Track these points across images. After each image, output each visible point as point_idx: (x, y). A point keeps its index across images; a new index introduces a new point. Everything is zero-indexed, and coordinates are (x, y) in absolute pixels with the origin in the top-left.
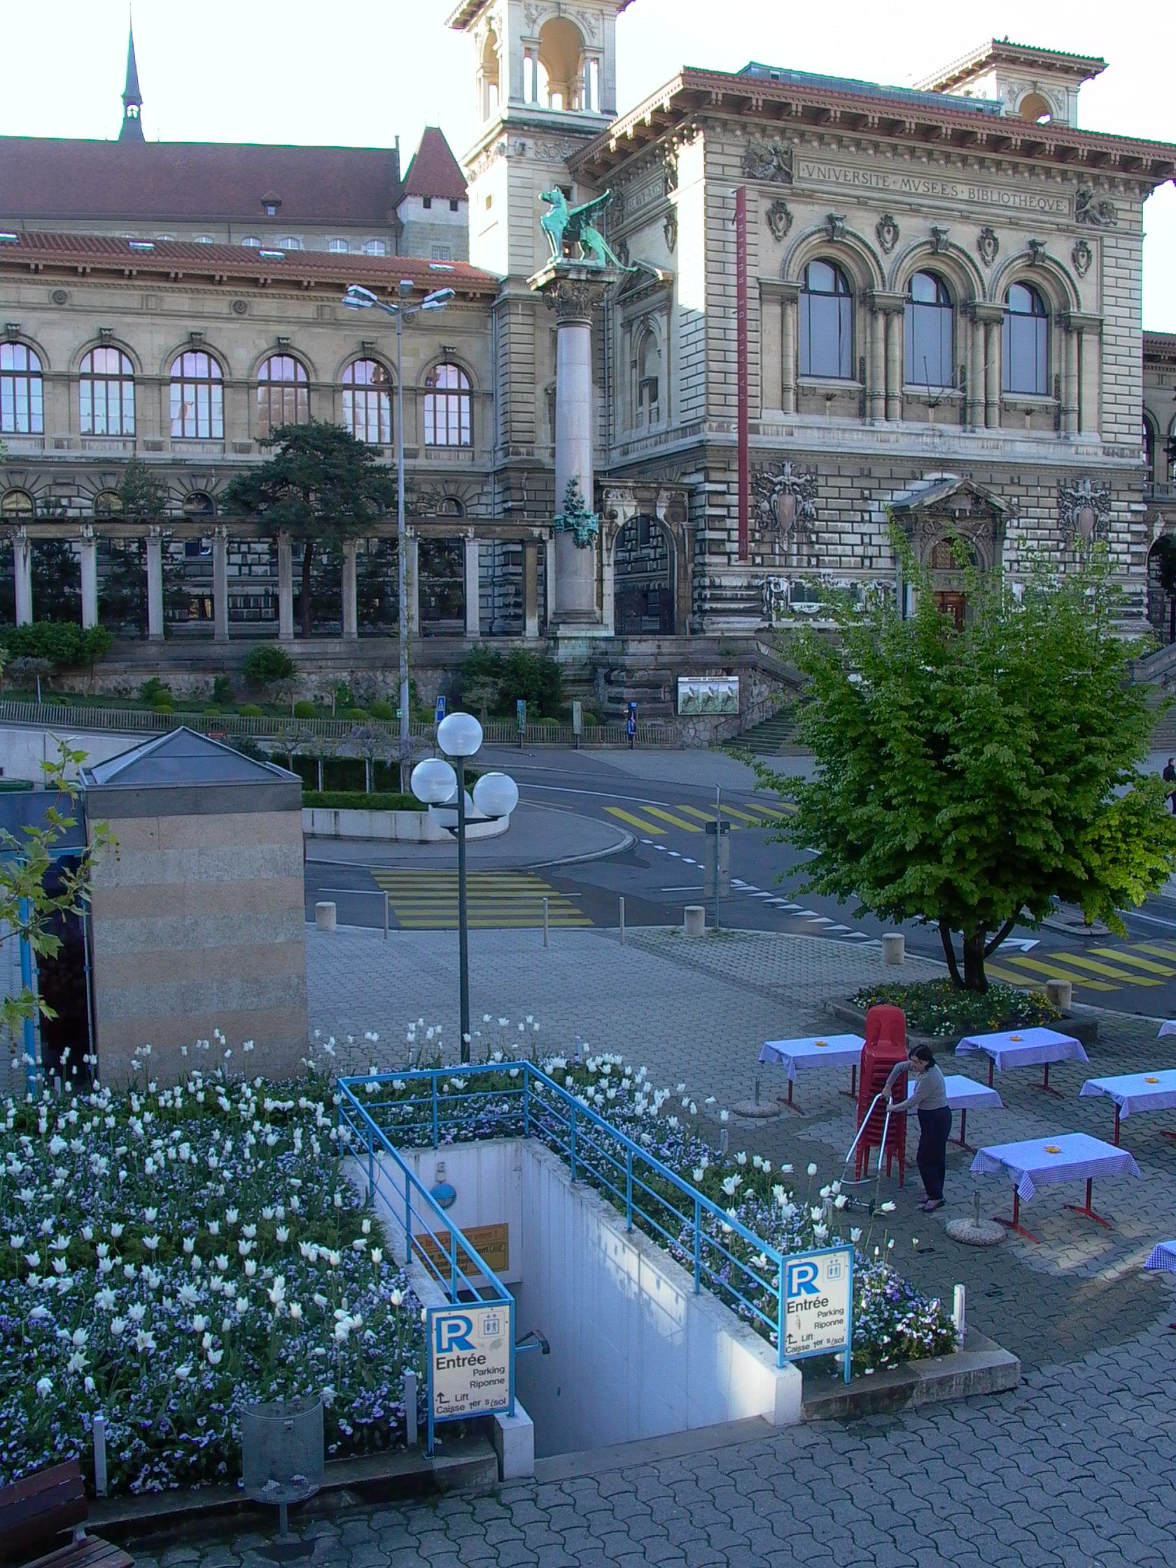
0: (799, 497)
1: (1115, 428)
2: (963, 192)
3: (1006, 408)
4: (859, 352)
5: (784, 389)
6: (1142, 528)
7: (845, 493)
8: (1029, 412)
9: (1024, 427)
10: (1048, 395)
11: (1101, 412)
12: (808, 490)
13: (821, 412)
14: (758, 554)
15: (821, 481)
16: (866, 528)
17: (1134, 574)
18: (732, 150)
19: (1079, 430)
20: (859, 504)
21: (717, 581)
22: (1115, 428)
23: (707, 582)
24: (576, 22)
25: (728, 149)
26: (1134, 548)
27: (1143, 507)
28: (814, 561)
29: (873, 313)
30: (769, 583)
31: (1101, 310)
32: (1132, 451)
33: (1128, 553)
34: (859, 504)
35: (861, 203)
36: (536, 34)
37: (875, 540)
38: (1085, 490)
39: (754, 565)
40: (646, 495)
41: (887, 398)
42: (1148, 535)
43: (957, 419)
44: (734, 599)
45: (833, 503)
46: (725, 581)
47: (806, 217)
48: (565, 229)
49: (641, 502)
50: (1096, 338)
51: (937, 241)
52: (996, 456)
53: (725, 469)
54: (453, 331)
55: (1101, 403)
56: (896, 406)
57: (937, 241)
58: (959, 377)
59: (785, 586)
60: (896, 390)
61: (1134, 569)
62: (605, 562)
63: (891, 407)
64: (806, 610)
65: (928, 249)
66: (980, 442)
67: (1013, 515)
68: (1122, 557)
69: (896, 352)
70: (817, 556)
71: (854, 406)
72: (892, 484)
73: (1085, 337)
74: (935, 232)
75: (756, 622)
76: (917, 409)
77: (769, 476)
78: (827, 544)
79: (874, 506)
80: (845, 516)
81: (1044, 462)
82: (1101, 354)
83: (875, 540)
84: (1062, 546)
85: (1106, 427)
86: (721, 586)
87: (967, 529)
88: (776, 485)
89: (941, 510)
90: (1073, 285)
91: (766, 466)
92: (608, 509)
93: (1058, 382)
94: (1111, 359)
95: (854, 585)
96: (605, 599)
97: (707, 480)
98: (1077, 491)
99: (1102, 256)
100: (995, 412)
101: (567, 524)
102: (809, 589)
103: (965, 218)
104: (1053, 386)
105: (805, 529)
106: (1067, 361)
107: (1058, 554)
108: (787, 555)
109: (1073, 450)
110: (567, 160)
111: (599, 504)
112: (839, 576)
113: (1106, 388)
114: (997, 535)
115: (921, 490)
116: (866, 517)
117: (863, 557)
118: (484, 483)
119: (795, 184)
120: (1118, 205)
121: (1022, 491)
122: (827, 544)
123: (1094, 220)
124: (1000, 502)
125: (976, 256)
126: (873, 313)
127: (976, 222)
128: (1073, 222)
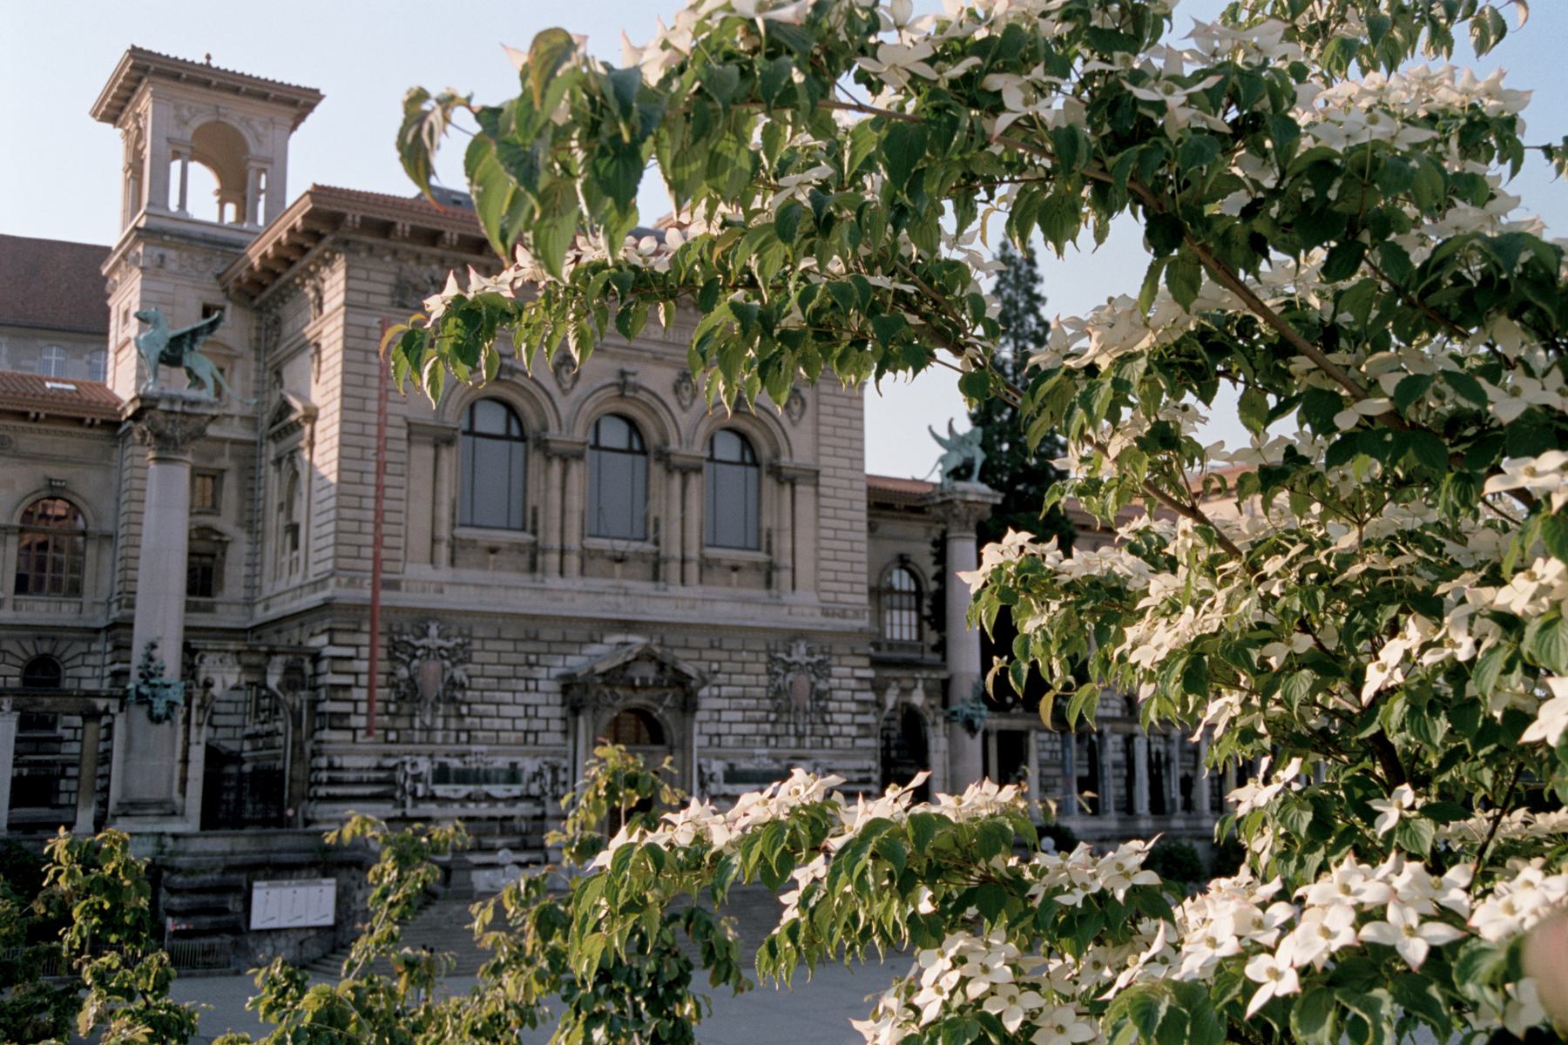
0: (447, 663)
1: (835, 586)
3: (706, 565)
4: (532, 500)
5: (434, 541)
6: (870, 696)
7: (506, 658)
8: (735, 569)
9: (729, 584)
10: (758, 549)
11: (818, 569)
12: (460, 655)
13: (483, 566)
14: (393, 729)
15: (476, 645)
16: (530, 698)
17: (861, 748)
18: (380, 277)
19: (794, 587)
20: (523, 671)
21: (337, 762)
22: (835, 586)
23: (323, 762)
24: (240, 128)
25: (373, 275)
26: (859, 719)
27: (870, 673)
28: (463, 737)
29: (548, 459)
30: (404, 763)
31: (817, 460)
32: (856, 612)
33: (852, 723)
34: (523, 671)
36: (188, 137)
37: (542, 712)
38: (799, 654)
39: (386, 741)
40: (254, 659)
41: (563, 552)
42: (880, 705)
43: (650, 574)
44: (359, 783)
45: (489, 670)
46: (348, 762)
48: (163, 353)
49: (247, 668)
50: (811, 490)
51: (624, 385)
52: (693, 617)
53: (355, 631)
54: (66, 461)
55: (818, 559)
56: (573, 562)
57: (624, 385)
58: (650, 529)
59: (424, 766)
60: (573, 542)
61: (859, 742)
62: (193, 738)
63: (566, 562)
64: (452, 795)
65: (614, 391)
67: (705, 683)
68: (846, 730)
69: (575, 501)
70: (468, 731)
71: (524, 560)
72: (565, 648)
73: (799, 488)
74: (623, 374)
75: (388, 809)
76: (600, 564)
77: (411, 639)
78: (481, 717)
79: (541, 673)
80: (505, 684)
81: (749, 623)
82: (818, 507)
83: (542, 712)
84: (772, 717)
85: (824, 585)
86: (341, 769)
87: (652, 699)
88: (417, 648)
89: (617, 676)
90: (784, 433)
91: (407, 627)
92: (201, 678)
93: (769, 536)
94: (830, 512)
95: (513, 765)
96: (189, 785)
97: (331, 643)
98: (789, 655)
99: (818, 403)
100: (693, 570)
101: (139, 695)
102: (457, 771)
103: (658, 359)
104: (764, 541)
105: (453, 700)
106: (779, 513)
107: (767, 728)
108: (430, 730)
109: (785, 610)
110: (218, 276)
111: (189, 670)
112: (495, 753)
113: (824, 543)
114: (688, 706)
115: (603, 654)
116: (532, 685)
117: (526, 732)
118: (90, 641)
121: (725, 655)
122: (481, 717)
124: (688, 668)
125: (671, 400)
126: (548, 459)
127: (672, 364)
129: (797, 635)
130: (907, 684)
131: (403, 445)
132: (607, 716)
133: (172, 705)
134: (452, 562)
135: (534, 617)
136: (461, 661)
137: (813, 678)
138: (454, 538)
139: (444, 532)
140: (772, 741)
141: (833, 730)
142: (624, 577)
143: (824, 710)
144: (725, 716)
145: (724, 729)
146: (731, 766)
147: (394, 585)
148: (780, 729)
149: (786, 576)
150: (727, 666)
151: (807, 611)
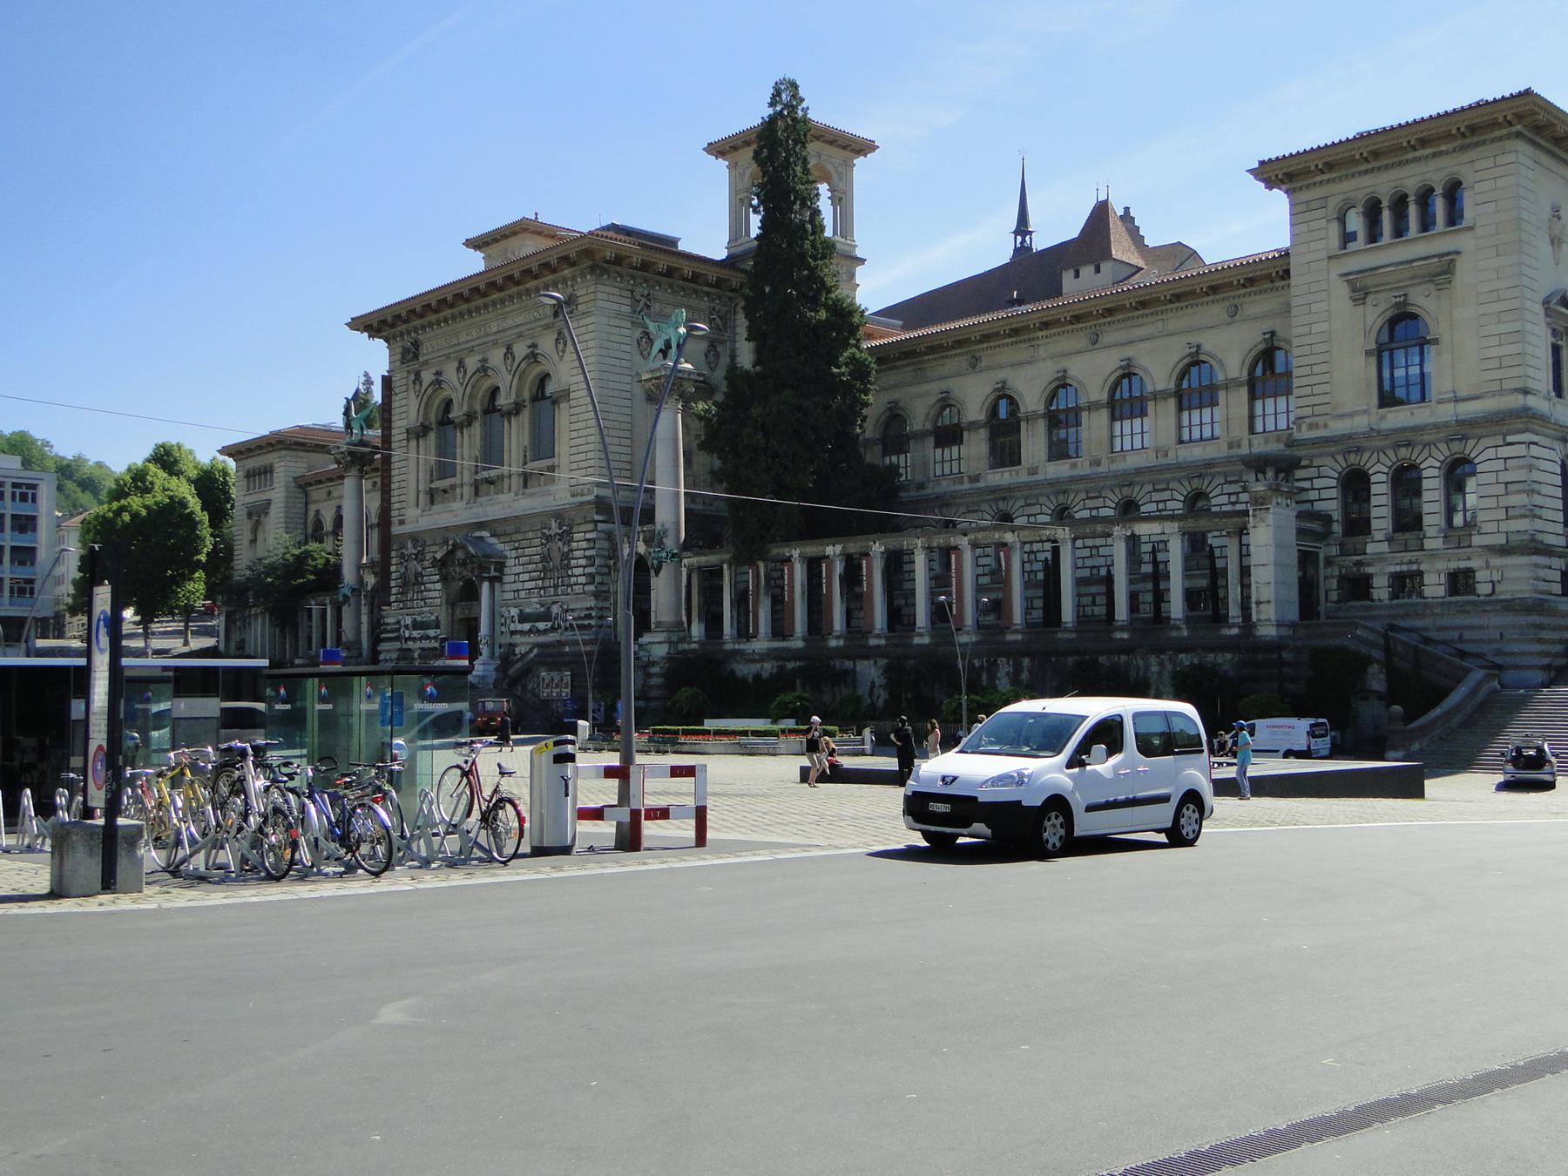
26: (588, 570)
47: (427, 376)
52: (508, 513)
59: (409, 621)
75: (397, 645)
103: (495, 343)
129: (558, 515)
133: (346, 598)
134: (432, 502)
135: (446, 528)
141: (573, 580)
143: (569, 567)
145: (520, 586)
147: (402, 522)
148: (547, 583)
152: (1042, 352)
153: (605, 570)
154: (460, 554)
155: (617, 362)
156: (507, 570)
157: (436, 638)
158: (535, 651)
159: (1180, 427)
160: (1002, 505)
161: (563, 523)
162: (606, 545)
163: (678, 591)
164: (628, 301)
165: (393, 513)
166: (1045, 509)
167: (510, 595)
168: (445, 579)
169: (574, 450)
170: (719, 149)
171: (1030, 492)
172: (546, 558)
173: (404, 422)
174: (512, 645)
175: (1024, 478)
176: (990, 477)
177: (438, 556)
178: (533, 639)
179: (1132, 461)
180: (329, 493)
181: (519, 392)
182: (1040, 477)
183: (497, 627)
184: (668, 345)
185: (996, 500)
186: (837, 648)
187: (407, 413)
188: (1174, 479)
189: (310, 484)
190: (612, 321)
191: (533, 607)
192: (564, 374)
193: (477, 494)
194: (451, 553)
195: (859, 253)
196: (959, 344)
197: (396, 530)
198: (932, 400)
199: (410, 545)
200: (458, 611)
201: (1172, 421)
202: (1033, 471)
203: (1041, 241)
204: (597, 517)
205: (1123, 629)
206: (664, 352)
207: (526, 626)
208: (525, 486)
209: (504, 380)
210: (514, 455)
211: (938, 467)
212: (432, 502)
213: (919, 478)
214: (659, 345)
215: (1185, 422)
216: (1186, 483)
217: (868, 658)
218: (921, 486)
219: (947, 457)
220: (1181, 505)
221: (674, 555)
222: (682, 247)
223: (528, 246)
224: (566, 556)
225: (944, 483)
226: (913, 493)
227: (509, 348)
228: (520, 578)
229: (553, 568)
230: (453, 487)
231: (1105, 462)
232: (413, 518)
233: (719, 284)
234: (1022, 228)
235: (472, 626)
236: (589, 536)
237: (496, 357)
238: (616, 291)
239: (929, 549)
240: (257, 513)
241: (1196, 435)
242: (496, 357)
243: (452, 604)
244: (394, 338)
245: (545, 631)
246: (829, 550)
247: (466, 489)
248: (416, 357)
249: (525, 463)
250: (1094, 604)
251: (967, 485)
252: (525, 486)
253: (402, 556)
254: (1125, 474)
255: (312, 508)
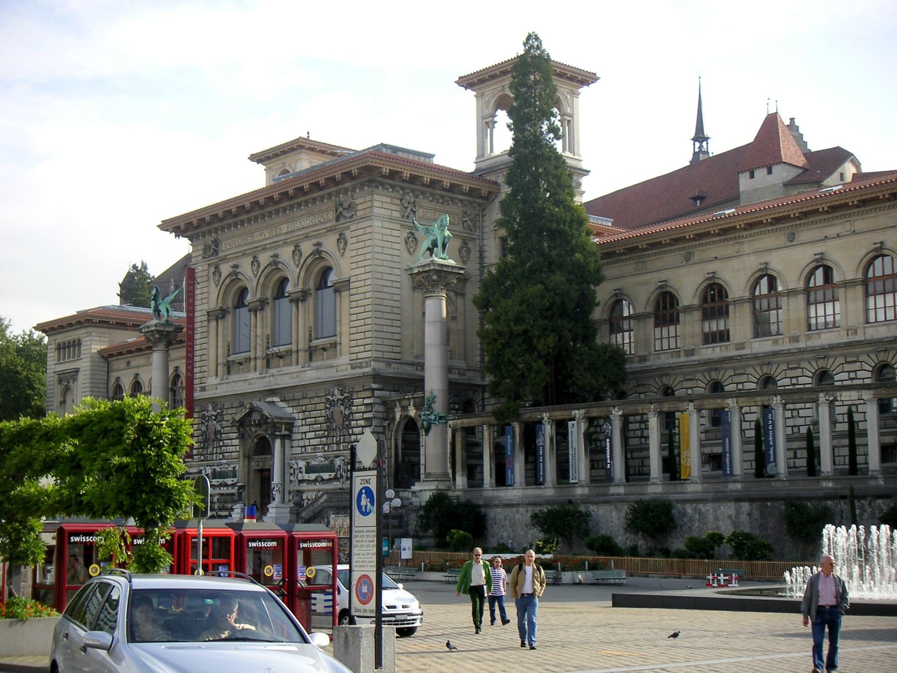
2: (284, 228)
9: (323, 359)
13: (238, 372)
32: (367, 363)
35: (244, 254)
47: (226, 269)
59: (209, 471)
66: (290, 376)
103: (285, 243)
109: (335, 370)
119: (220, 255)
120: (358, 201)
123: (345, 217)
128: (334, 223)
129: (340, 383)
130: (405, 403)
131: (205, 323)
132: (251, 443)
134: (229, 373)
135: (242, 394)
136: (220, 421)
137: (342, 408)
138: (228, 361)
139: (220, 360)
140: (326, 448)
142: (284, 365)
143: (350, 427)
144: (309, 435)
145: (307, 442)
146: (308, 463)
147: (203, 389)
149: (338, 347)
150: (309, 407)
151: (344, 368)
152: (747, 248)
153: (381, 429)
154: (256, 417)
155: (389, 258)
156: (295, 430)
157: (233, 485)
158: (325, 497)
159: (867, 310)
160: (714, 375)
161: (345, 388)
162: (381, 408)
163: (445, 447)
164: (398, 208)
165: (196, 382)
166: (752, 378)
167: (298, 450)
168: (242, 437)
169: (353, 330)
170: (469, 82)
171: (737, 363)
172: (329, 420)
173: (205, 307)
174: (300, 493)
175: (733, 353)
176: (703, 351)
177: (238, 418)
178: (318, 486)
179: (827, 338)
180: (128, 363)
181: (305, 282)
182: (746, 351)
183: (287, 476)
184: (434, 244)
185: (709, 371)
186: (582, 495)
187: (209, 297)
188: (862, 353)
189: (112, 355)
190: (386, 225)
191: (319, 460)
192: (344, 267)
193: (268, 366)
194: (249, 414)
195: (584, 166)
196: (676, 241)
197: (197, 395)
198: (652, 288)
199: (210, 408)
200: (253, 464)
201: (860, 304)
202: (740, 346)
203: (716, 147)
204: (374, 386)
205: (827, 479)
206: (431, 250)
207: (313, 476)
208: (311, 359)
209: (292, 271)
210: (301, 334)
211: (658, 343)
212: (229, 373)
213: (642, 353)
214: (427, 244)
215: (871, 305)
216: (873, 356)
217: (608, 502)
218: (643, 359)
219: (665, 334)
220: (869, 374)
221: (441, 418)
222: (436, 161)
223: (304, 163)
224: (347, 418)
225: (663, 356)
226: (636, 366)
227: (297, 246)
228: (306, 435)
229: (337, 427)
230: (248, 360)
231: (802, 338)
232: (213, 384)
233: (472, 192)
234: (700, 136)
235: (265, 476)
236: (367, 401)
237: (286, 254)
238: (389, 200)
239: (660, 413)
240: (67, 379)
241: (881, 317)
242: (286, 254)
243: (248, 457)
244: (197, 238)
245: (330, 480)
246: (577, 413)
247: (259, 362)
248: (216, 252)
249: (310, 341)
250: (795, 457)
251: (683, 359)
252: (311, 359)
253: (204, 417)
254: (822, 348)
255: (114, 375)
